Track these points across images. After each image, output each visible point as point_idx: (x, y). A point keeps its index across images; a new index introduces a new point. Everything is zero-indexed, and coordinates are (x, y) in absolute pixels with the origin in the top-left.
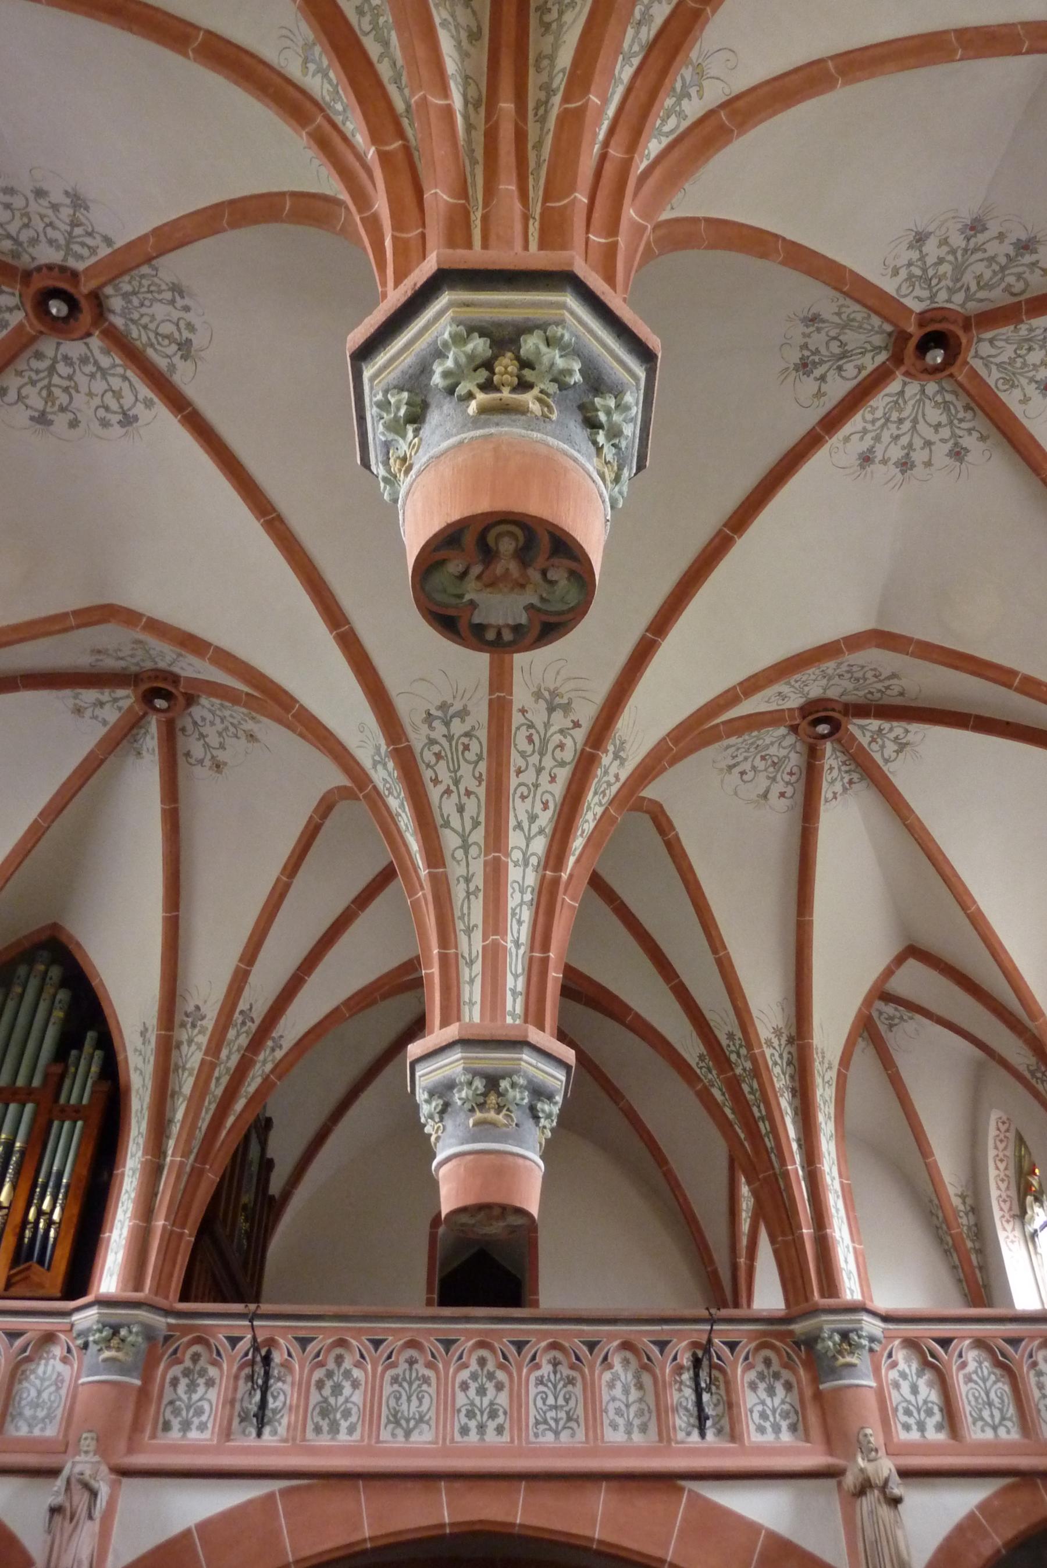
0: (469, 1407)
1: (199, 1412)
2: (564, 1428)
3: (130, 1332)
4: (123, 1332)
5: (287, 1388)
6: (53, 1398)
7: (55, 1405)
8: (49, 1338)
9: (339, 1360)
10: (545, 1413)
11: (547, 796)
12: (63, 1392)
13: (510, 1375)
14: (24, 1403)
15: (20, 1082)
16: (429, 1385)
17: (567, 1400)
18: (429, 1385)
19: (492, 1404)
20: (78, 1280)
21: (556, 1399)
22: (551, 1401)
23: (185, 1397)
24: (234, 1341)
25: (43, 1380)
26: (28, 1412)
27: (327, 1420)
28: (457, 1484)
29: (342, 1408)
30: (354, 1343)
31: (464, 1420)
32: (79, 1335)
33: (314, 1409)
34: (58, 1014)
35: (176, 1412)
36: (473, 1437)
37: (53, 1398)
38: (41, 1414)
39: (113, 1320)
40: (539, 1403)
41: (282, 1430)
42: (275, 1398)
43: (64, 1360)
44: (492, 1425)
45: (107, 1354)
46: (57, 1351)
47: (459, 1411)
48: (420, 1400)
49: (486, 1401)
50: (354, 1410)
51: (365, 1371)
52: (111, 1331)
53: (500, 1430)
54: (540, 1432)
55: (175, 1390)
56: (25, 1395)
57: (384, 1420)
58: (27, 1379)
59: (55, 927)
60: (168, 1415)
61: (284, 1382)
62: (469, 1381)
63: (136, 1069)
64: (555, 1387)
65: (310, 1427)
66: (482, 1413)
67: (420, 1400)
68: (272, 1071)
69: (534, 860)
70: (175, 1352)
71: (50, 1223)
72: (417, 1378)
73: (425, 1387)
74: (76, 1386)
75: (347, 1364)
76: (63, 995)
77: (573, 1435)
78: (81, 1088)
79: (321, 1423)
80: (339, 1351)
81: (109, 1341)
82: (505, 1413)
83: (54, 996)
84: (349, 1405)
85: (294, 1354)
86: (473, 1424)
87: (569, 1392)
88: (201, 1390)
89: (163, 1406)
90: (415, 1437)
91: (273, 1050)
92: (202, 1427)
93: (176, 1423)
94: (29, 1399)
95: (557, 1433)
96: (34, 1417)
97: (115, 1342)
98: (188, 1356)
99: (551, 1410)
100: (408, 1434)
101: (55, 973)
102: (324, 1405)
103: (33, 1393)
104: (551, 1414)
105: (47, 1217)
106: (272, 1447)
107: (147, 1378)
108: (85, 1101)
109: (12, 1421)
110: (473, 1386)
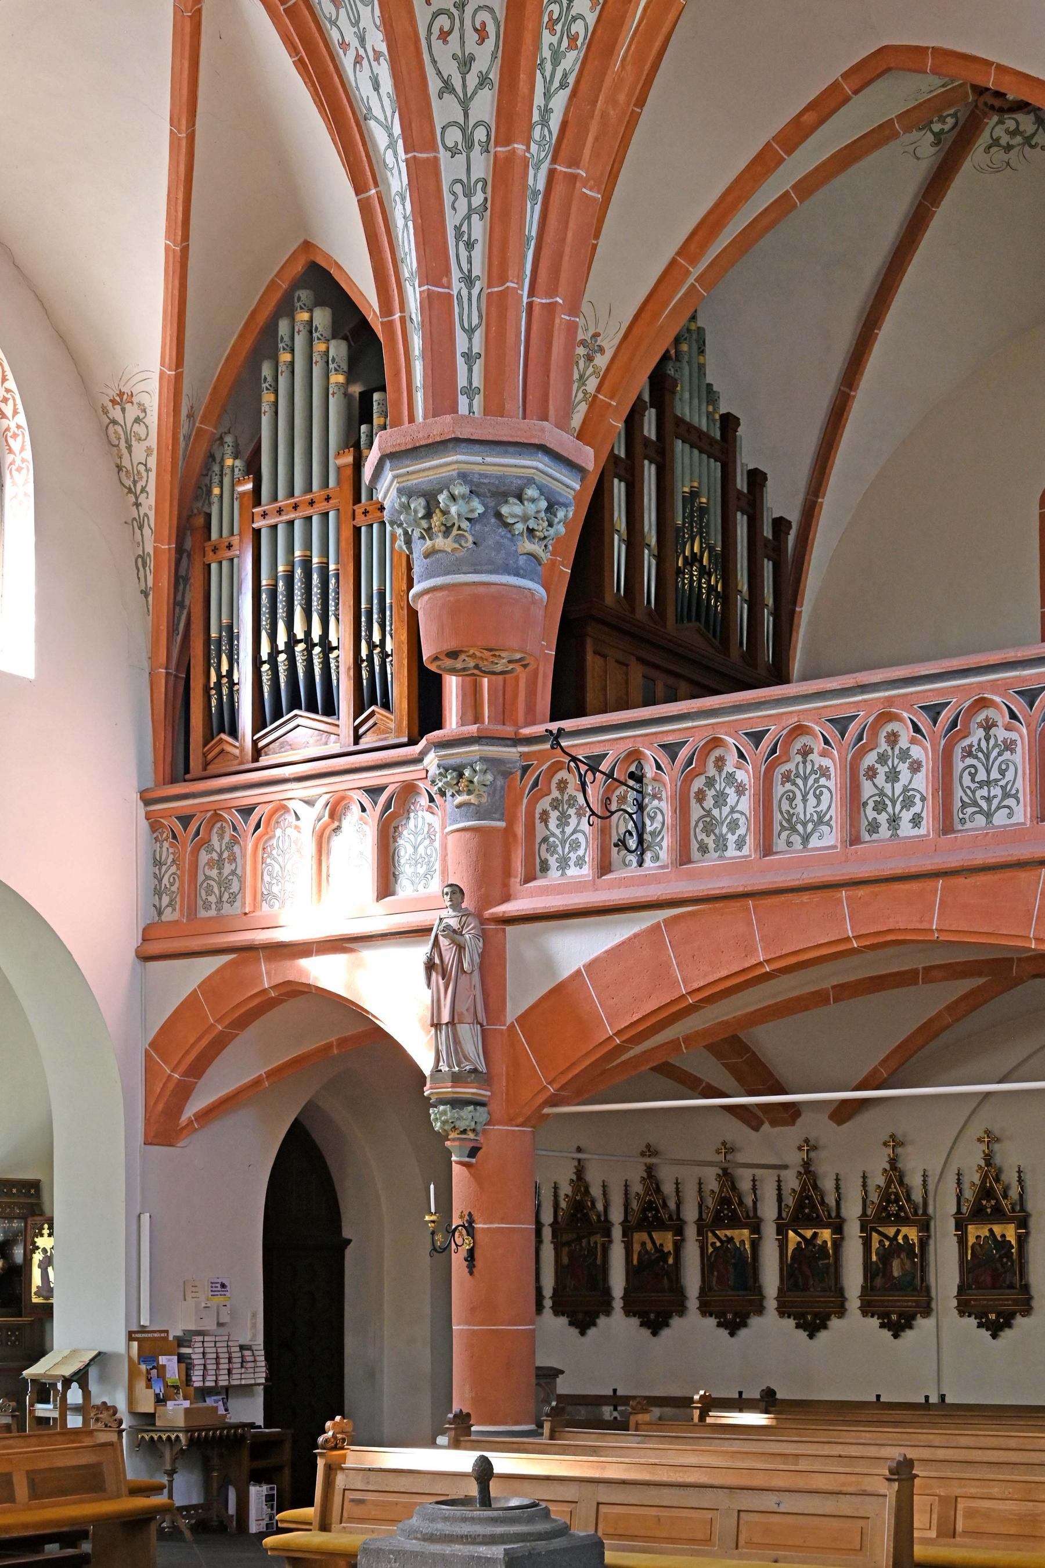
0: (877, 798)
1: (575, 846)
2: (998, 808)
3: (475, 771)
4: (467, 773)
5: (663, 805)
8: (409, 790)
9: (720, 763)
10: (973, 792)
11: (484, 16)
12: (437, 844)
13: (925, 749)
14: (403, 861)
16: (828, 778)
17: (1002, 772)
18: (828, 778)
19: (906, 789)
21: (988, 772)
22: (982, 776)
23: (557, 832)
25: (415, 834)
27: (713, 837)
28: (861, 892)
29: (728, 821)
30: (730, 740)
31: (871, 814)
33: (696, 826)
35: (552, 850)
36: (884, 832)
38: (422, 870)
39: (452, 761)
40: (967, 780)
41: (663, 854)
42: (652, 819)
43: (430, 810)
44: (906, 816)
45: (459, 799)
47: (865, 804)
48: (818, 797)
49: (899, 788)
50: (742, 821)
51: (747, 771)
52: (455, 774)
53: (916, 821)
54: (966, 817)
55: (547, 826)
56: (402, 853)
57: (777, 827)
58: (400, 834)
60: (544, 855)
61: (660, 799)
62: (877, 766)
64: (987, 758)
65: (694, 846)
66: (894, 803)
67: (818, 797)
68: (599, 389)
69: (480, 134)
70: (536, 784)
72: (813, 771)
73: (823, 781)
75: (729, 768)
77: (1010, 815)
79: (706, 840)
80: (717, 752)
82: (923, 799)
84: (736, 816)
86: (883, 818)
87: (1006, 762)
88: (573, 821)
89: (537, 846)
90: (814, 842)
91: (590, 358)
92: (580, 862)
93: (552, 861)
94: (407, 857)
95: (989, 815)
97: (463, 784)
98: (554, 785)
99: (981, 787)
100: (806, 839)
102: (708, 819)
104: (984, 792)
106: (654, 873)
110: (882, 770)
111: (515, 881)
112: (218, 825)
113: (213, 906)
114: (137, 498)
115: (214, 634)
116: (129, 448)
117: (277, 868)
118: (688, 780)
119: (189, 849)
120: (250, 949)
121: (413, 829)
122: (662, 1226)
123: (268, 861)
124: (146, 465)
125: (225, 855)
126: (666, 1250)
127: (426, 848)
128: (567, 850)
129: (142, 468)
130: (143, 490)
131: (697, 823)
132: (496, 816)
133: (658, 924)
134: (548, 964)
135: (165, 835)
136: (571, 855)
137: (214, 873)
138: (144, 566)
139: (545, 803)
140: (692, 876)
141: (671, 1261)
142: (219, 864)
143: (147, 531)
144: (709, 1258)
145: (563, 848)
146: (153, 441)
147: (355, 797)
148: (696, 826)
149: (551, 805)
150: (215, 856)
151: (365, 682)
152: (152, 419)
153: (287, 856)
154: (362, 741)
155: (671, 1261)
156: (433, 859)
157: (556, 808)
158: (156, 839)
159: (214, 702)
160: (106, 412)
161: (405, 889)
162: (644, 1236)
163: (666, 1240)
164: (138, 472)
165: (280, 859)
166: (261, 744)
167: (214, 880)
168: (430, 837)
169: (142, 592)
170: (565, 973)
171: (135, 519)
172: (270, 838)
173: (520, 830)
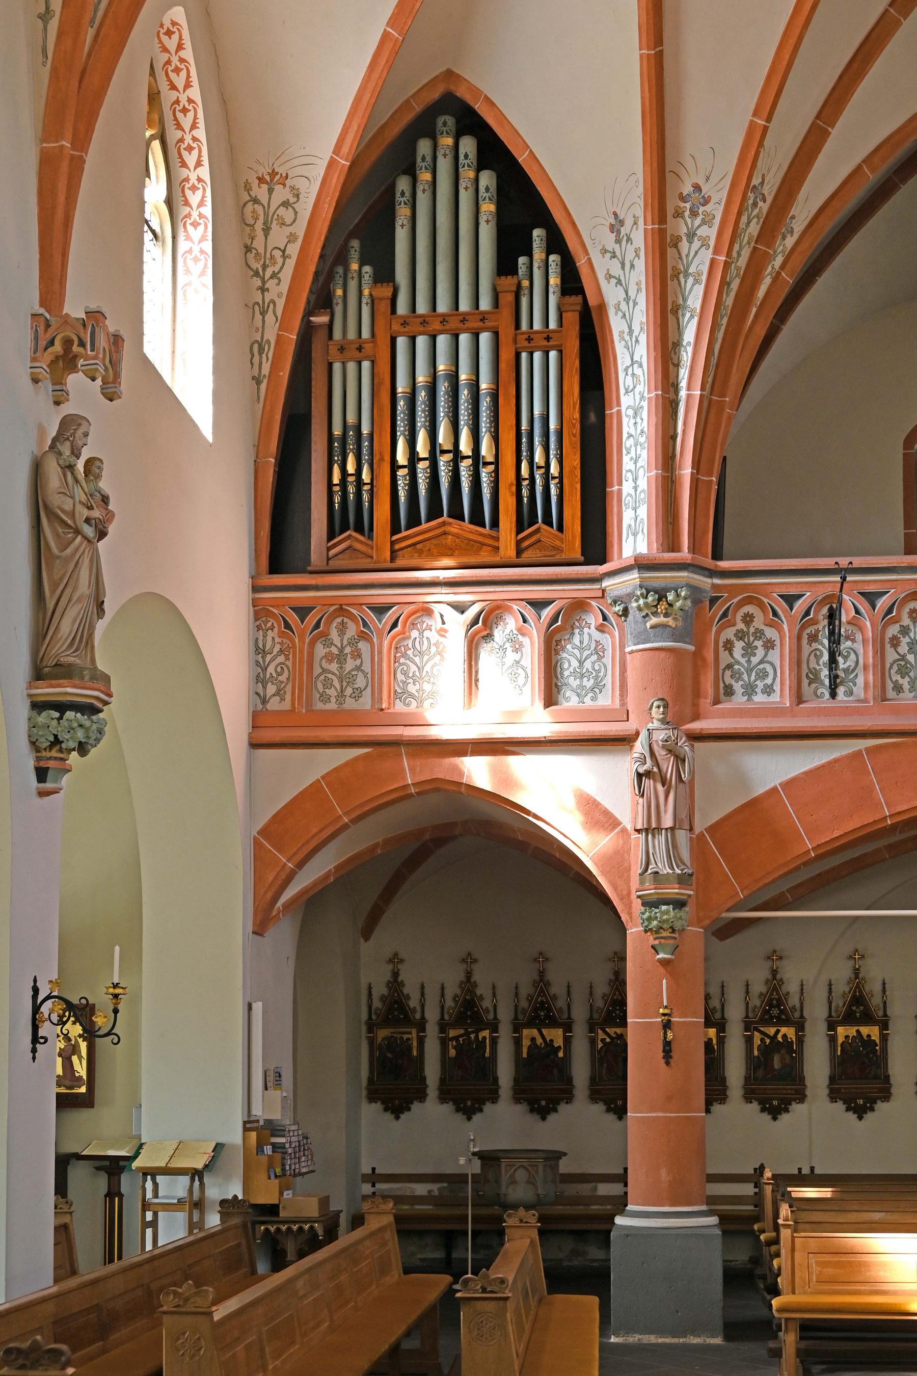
1: (763, 675)
6: (597, 668)
7: (602, 674)
8: (579, 606)
12: (608, 660)
14: (566, 673)
15: (465, 306)
20: (596, 545)
24: (790, 600)
25: (581, 650)
26: (574, 682)
32: (615, 602)
34: (488, 208)
35: (737, 676)
37: (597, 668)
38: (589, 684)
42: (846, 658)
43: (600, 629)
46: (593, 619)
55: (731, 655)
56: (566, 666)
58: (563, 648)
59: (449, 74)
60: (728, 680)
61: (853, 641)
63: (609, 277)
65: (890, 685)
70: (725, 615)
71: (547, 477)
74: (623, 654)
76: (487, 179)
78: (544, 308)
83: (477, 180)
85: (863, 611)
88: (760, 652)
89: (721, 672)
92: (768, 690)
93: (737, 687)
94: (571, 669)
96: (582, 687)
101: (468, 145)
102: (903, 663)
103: (575, 663)
105: (543, 470)
107: (700, 645)
108: (553, 325)
109: (559, 692)
111: (706, 703)
112: (339, 620)
113: (333, 700)
114: (264, 282)
115: (337, 431)
117: (413, 668)
118: (885, 627)
119: (307, 640)
120: (395, 743)
121: (578, 643)
122: (553, 1023)
123: (402, 660)
124: (284, 252)
125: (348, 650)
126: (556, 1045)
127: (593, 663)
128: (753, 678)
129: (278, 254)
130: (274, 275)
131: (892, 665)
132: (687, 640)
133: (860, 752)
134: (742, 780)
135: (269, 624)
136: (758, 682)
137: (334, 667)
138: (260, 354)
139: (729, 633)
140: (897, 711)
141: (561, 1054)
142: (341, 658)
143: (270, 317)
144: (600, 1052)
145: (749, 676)
147: (515, 607)
148: (891, 668)
149: (735, 635)
150: (335, 650)
151: (525, 499)
153: (426, 658)
154: (523, 556)
155: (561, 1054)
156: (602, 674)
157: (741, 639)
159: (337, 499)
161: (570, 701)
162: (535, 1032)
163: (556, 1036)
164: (272, 257)
165: (417, 659)
166: (397, 547)
167: (333, 674)
168: (599, 651)
169: (253, 378)
170: (760, 790)
171: (258, 303)
172: (404, 639)
173: (710, 656)
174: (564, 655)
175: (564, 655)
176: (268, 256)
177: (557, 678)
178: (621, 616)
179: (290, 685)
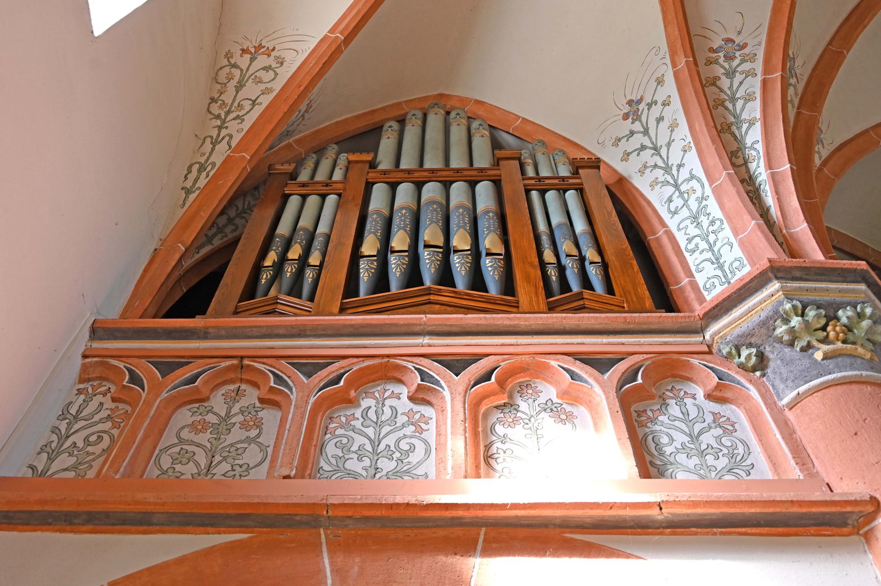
4: (844, 315)
56: (665, 440)
81: (824, 329)
116: (239, 87)
119: (164, 395)
129: (247, 105)
143: (222, 147)
146: (278, 86)
150: (212, 418)
152: (286, 72)
156: (741, 449)
158: (80, 392)
160: (228, 55)
165: (370, 432)
171: (211, 137)
174: (657, 428)
175: (657, 428)
176: (236, 104)
177: (651, 455)
178: (754, 369)
179: (102, 459)
